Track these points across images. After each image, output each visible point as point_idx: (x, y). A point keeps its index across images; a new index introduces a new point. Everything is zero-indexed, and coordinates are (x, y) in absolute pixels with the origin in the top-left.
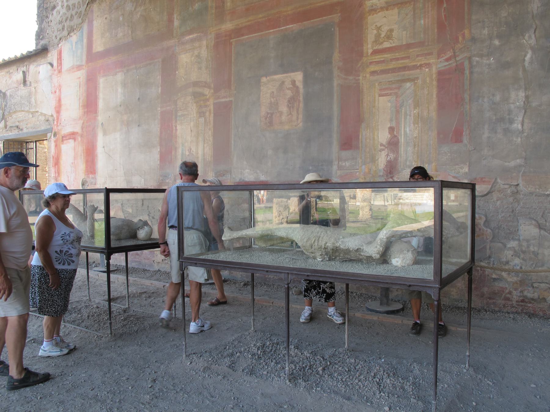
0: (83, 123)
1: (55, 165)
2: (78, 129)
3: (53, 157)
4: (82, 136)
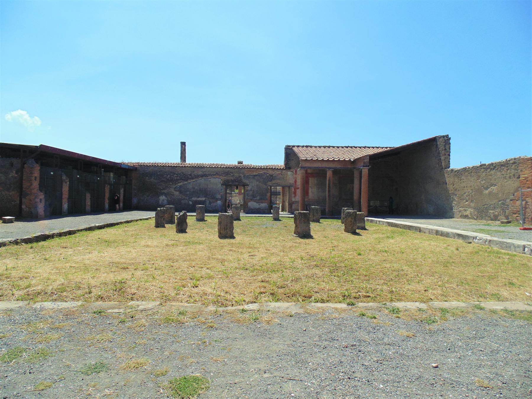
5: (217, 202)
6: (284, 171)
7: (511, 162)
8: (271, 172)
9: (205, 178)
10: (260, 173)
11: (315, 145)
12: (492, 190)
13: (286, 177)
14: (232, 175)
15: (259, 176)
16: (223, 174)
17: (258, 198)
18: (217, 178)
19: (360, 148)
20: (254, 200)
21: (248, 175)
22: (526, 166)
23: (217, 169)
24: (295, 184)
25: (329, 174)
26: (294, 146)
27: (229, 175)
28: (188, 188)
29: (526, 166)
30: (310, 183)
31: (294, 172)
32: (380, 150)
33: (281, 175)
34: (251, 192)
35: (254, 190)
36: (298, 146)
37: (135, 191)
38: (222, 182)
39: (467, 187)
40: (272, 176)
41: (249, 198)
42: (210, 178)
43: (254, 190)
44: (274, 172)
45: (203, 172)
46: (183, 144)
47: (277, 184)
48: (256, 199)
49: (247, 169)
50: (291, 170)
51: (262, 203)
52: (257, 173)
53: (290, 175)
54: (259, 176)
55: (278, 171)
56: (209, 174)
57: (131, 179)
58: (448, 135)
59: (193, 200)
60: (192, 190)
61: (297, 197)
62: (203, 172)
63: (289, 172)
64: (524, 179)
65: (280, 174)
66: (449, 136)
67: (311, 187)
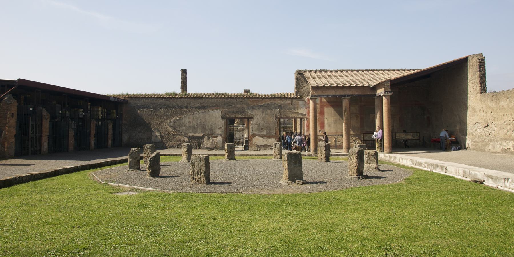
0: (319, 117)
1: (307, 127)
3: (306, 125)
6: (294, 100)
8: (279, 102)
10: (266, 103)
11: (331, 69)
14: (234, 106)
15: (266, 106)
16: (223, 106)
19: (383, 71)
20: (259, 134)
21: (252, 105)
23: (217, 99)
24: (308, 115)
25: (345, 103)
26: (305, 71)
27: (231, 106)
28: (184, 122)
30: (326, 114)
32: (406, 73)
33: (291, 105)
34: (256, 125)
35: (259, 124)
36: (310, 71)
37: (126, 127)
43: (259, 124)
44: (282, 101)
45: (201, 103)
46: (184, 72)
49: (251, 99)
52: (263, 104)
53: (302, 104)
54: (266, 106)
55: (287, 100)
56: (207, 106)
57: (122, 113)
58: (482, 54)
59: (190, 136)
60: (188, 125)
62: (201, 103)
63: (300, 101)
65: (290, 104)
66: (483, 54)
67: (327, 118)
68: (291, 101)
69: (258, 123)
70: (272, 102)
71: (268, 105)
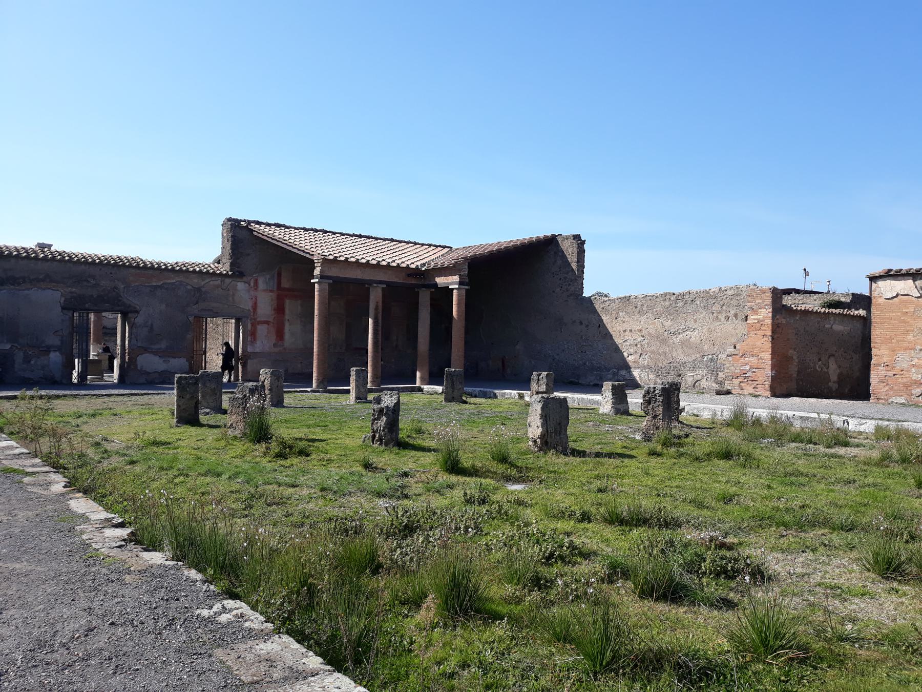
1: (251, 335)
2: (271, 320)
4: (273, 323)
5: (48, 355)
6: (228, 281)
7: (730, 293)
8: (196, 281)
9: (12, 287)
10: (169, 281)
12: (688, 337)
13: (234, 295)
14: (93, 282)
17: (163, 345)
18: (49, 289)
21: (137, 284)
22: (761, 301)
27: (85, 283)
29: (761, 301)
30: (287, 311)
31: (252, 284)
35: (152, 325)
38: (63, 299)
39: (631, 331)
40: (199, 290)
41: (140, 344)
42: (28, 289)
43: (152, 325)
44: (203, 280)
47: (212, 310)
48: (157, 346)
50: (245, 279)
51: (175, 358)
55: (213, 279)
61: (258, 342)
63: (239, 284)
64: (756, 321)
65: (218, 286)
68: (221, 282)
69: (150, 323)
70: (181, 281)
71: (174, 286)
